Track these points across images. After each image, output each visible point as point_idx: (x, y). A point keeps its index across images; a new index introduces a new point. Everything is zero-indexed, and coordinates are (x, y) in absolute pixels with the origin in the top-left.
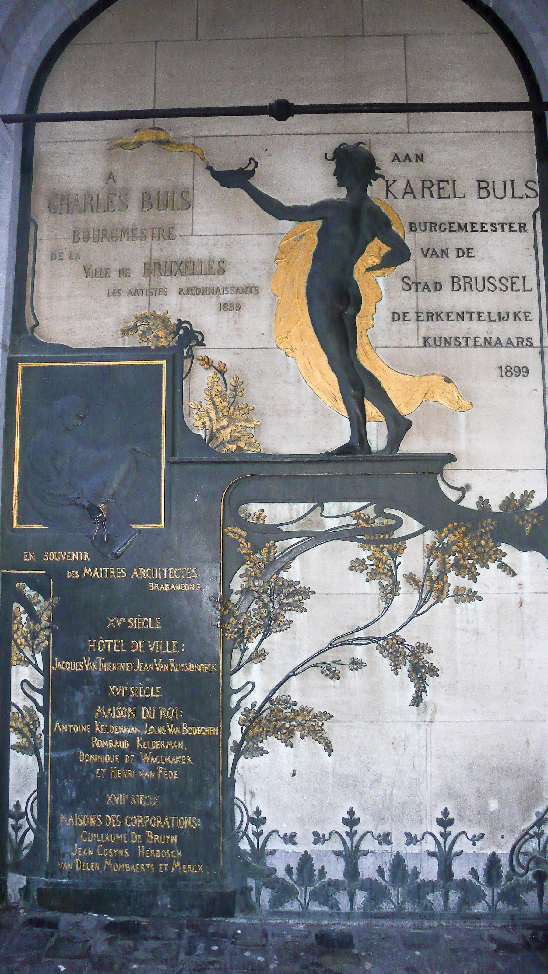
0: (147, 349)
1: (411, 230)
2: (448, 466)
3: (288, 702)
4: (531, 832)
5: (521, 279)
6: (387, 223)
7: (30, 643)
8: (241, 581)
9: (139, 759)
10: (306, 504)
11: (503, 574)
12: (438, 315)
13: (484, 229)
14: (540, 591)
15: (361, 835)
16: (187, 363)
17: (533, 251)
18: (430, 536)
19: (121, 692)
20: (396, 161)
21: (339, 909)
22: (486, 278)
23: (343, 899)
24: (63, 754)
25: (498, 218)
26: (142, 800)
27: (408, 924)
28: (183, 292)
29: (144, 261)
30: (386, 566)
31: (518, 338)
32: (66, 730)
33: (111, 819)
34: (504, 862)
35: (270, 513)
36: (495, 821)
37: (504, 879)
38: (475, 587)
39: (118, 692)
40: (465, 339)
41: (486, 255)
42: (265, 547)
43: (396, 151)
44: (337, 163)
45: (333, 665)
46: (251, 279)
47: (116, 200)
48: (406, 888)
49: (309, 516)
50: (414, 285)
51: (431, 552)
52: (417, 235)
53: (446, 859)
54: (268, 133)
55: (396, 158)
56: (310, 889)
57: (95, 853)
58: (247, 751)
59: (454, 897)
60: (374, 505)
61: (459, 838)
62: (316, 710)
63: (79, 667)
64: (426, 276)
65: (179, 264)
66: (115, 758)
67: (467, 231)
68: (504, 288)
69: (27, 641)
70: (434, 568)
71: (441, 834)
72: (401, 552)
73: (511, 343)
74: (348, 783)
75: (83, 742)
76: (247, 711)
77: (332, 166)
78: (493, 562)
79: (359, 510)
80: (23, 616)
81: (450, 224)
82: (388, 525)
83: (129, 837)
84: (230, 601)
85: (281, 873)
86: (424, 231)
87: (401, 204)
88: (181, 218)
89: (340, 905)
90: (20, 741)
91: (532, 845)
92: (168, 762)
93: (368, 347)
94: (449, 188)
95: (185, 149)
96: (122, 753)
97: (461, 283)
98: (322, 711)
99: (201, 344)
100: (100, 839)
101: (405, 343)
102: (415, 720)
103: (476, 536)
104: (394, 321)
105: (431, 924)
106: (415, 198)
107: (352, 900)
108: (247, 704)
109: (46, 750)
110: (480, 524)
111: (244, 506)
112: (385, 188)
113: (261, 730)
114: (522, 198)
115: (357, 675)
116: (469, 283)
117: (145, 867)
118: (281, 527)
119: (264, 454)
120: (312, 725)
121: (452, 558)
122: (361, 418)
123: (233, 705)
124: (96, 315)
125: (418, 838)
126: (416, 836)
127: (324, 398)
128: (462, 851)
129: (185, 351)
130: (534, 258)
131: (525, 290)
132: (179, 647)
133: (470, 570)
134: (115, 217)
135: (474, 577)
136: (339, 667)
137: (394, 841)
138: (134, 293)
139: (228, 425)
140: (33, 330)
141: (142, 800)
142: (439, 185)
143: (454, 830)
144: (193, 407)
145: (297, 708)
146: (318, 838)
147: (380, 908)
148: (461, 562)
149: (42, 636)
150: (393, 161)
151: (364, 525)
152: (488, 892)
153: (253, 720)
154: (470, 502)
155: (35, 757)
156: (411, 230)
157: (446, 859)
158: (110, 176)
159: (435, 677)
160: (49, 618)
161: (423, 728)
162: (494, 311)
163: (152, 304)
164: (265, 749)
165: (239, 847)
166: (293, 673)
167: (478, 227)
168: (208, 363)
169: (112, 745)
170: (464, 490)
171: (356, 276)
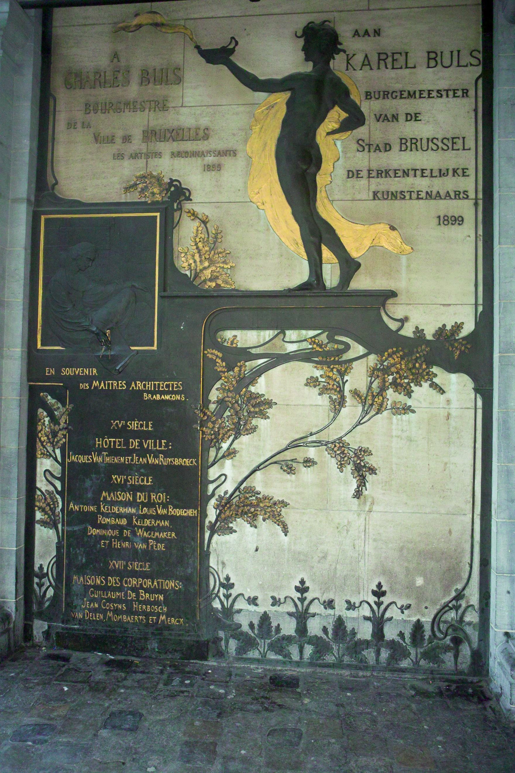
0: (145, 203)
1: (366, 99)
2: (390, 301)
3: (251, 490)
4: (450, 605)
6: (347, 92)
7: (51, 440)
8: (217, 393)
9: (134, 533)
11: (434, 392)
12: (387, 172)
13: (431, 96)
14: (465, 406)
15: (309, 600)
16: (177, 215)
17: (473, 114)
18: (372, 359)
19: (121, 480)
20: (356, 37)
21: (291, 659)
22: (430, 139)
23: (294, 652)
24: (76, 528)
25: (443, 85)
26: (136, 566)
27: (346, 673)
29: (142, 128)
30: (335, 383)
31: (455, 192)
32: (78, 510)
33: (112, 580)
34: (427, 628)
35: (242, 339)
36: (420, 595)
37: (426, 643)
38: (409, 402)
39: (119, 480)
40: (409, 193)
41: (431, 119)
42: (237, 366)
43: (357, 27)
44: (305, 40)
45: (290, 463)
46: (231, 144)
48: (346, 645)
49: (273, 341)
50: (367, 146)
51: (373, 372)
52: (372, 103)
53: (379, 623)
54: (247, 14)
55: (356, 33)
57: (100, 605)
58: (220, 529)
59: (385, 654)
60: (327, 333)
61: (390, 607)
62: (276, 499)
63: (88, 460)
65: (171, 131)
66: (116, 532)
67: (415, 98)
68: (445, 148)
69: (48, 439)
70: (375, 385)
71: (375, 603)
72: (348, 372)
73: (450, 196)
74: (299, 558)
76: (221, 498)
77: (301, 42)
78: (426, 381)
79: (314, 337)
81: (401, 91)
82: (338, 350)
83: (126, 595)
84: (208, 409)
85: (245, 628)
86: (378, 99)
87: (359, 74)
88: (174, 91)
89: (291, 655)
90: (43, 517)
91: (451, 615)
92: (157, 536)
93: (326, 201)
94: (402, 60)
95: (177, 30)
96: (121, 528)
97: (408, 144)
98: (281, 499)
99: (189, 199)
100: (104, 595)
102: (356, 509)
103: (412, 360)
104: (348, 177)
105: (365, 674)
106: (371, 69)
107: (301, 652)
108: (220, 492)
109: (63, 525)
110: (415, 350)
111: (221, 333)
113: (231, 513)
114: (467, 66)
115: (309, 472)
116: (415, 144)
117: (139, 619)
118: (250, 350)
119: (237, 290)
120: (272, 510)
121: (391, 377)
122: (318, 261)
123: (210, 492)
124: (103, 176)
125: (357, 605)
126: (354, 603)
127: (287, 243)
128: (392, 617)
129: (175, 205)
130: (473, 120)
131: (464, 149)
132: (167, 446)
133: (405, 387)
134: (119, 92)
135: (409, 394)
136: (294, 465)
137: (336, 607)
138: (135, 156)
140: (53, 189)
141: (136, 566)
142: (393, 57)
143: (386, 600)
144: (181, 251)
145: (260, 496)
146: (275, 602)
147: (324, 659)
148: (398, 381)
150: (354, 37)
151: (318, 349)
152: (413, 651)
153: (225, 504)
154: (408, 331)
156: (366, 99)
157: (379, 623)
158: (115, 56)
159: (374, 475)
160: (66, 421)
161: (363, 517)
162: (436, 168)
164: (234, 528)
165: (212, 606)
166: (257, 469)
167: (425, 94)
168: (194, 215)
169: (113, 522)
170: (403, 321)
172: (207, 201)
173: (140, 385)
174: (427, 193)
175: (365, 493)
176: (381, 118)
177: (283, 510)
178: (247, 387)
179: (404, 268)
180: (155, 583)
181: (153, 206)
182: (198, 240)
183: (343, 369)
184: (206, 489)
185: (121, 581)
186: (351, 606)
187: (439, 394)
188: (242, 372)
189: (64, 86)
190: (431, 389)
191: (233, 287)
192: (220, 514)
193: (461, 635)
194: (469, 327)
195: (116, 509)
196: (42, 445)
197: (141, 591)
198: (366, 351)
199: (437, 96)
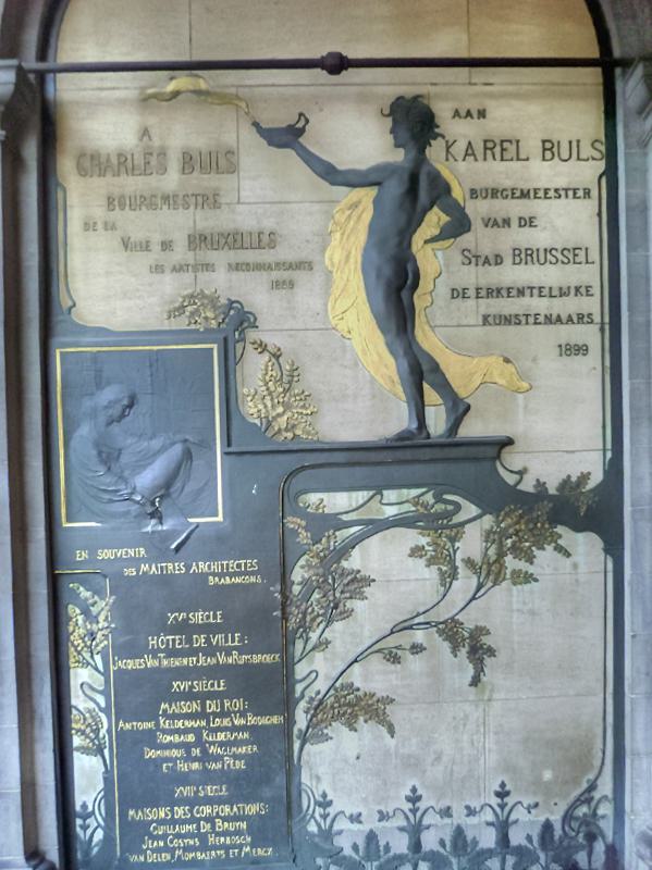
1: (472, 198)
2: (507, 449)
5: (584, 251)
6: (448, 189)
7: (89, 643)
8: (301, 570)
10: (365, 493)
11: (559, 556)
12: (499, 291)
16: (239, 346)
17: (597, 219)
20: (457, 118)
25: (561, 182)
26: (210, 790)
28: (237, 267)
31: (578, 315)
33: (180, 812)
36: (547, 789)
38: (531, 570)
44: (394, 120)
45: (394, 650)
46: (303, 255)
47: (154, 161)
51: (488, 536)
55: (457, 114)
56: (375, 864)
57: (165, 843)
62: (379, 695)
64: (486, 249)
67: (529, 198)
68: (566, 261)
69: (84, 642)
70: (492, 552)
71: (499, 805)
73: (572, 320)
75: (150, 739)
76: (312, 699)
77: (389, 122)
78: (549, 544)
80: (79, 617)
81: (513, 189)
84: (291, 592)
85: (348, 852)
87: (462, 166)
88: (224, 182)
90: (83, 743)
91: (583, 810)
93: (427, 328)
96: (187, 746)
97: (523, 256)
98: (385, 695)
104: (453, 297)
111: (304, 496)
112: (445, 149)
124: (138, 295)
127: (381, 381)
129: (237, 333)
131: (587, 262)
133: (526, 552)
135: (530, 559)
136: (399, 652)
137: (454, 814)
138: (179, 269)
139: (284, 412)
141: (210, 790)
143: (510, 800)
145: (360, 693)
146: (383, 816)
149: (99, 636)
150: (454, 117)
151: (422, 510)
153: (318, 707)
154: (528, 485)
155: (99, 756)
156: (472, 198)
157: (503, 827)
158: (145, 132)
160: (107, 617)
162: (555, 285)
163: (198, 281)
166: (356, 661)
167: (541, 194)
168: (262, 347)
170: (521, 473)
171: (414, 248)
173: (203, 567)
174: (546, 316)
175: (484, 679)
176: (491, 223)
177: (388, 707)
178: (338, 561)
179: (521, 410)
180: (235, 809)
181: (207, 335)
182: (267, 378)
183: (453, 534)
184: (293, 691)
185: (191, 811)
186: (471, 812)
187: (564, 558)
188: (332, 543)
189: (75, 171)
190: (556, 553)
191: (315, 439)
192: (311, 720)
193: (595, 830)
194: (597, 477)
195: (179, 724)
196: (76, 650)
197: (217, 820)
198: (479, 511)
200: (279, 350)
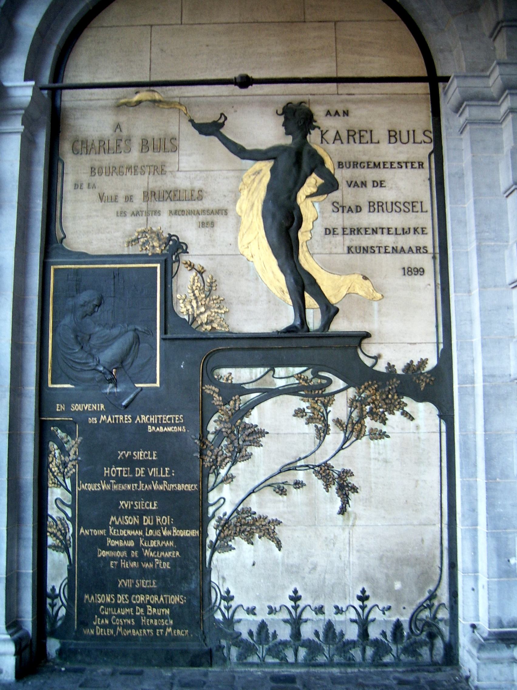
25: (402, 158)
41: (394, 186)
68: (407, 210)
93: (307, 254)
97: (376, 206)
101: (334, 250)
163: (149, 222)
172: (202, 253)
199: (398, 167)
200: (203, 268)
